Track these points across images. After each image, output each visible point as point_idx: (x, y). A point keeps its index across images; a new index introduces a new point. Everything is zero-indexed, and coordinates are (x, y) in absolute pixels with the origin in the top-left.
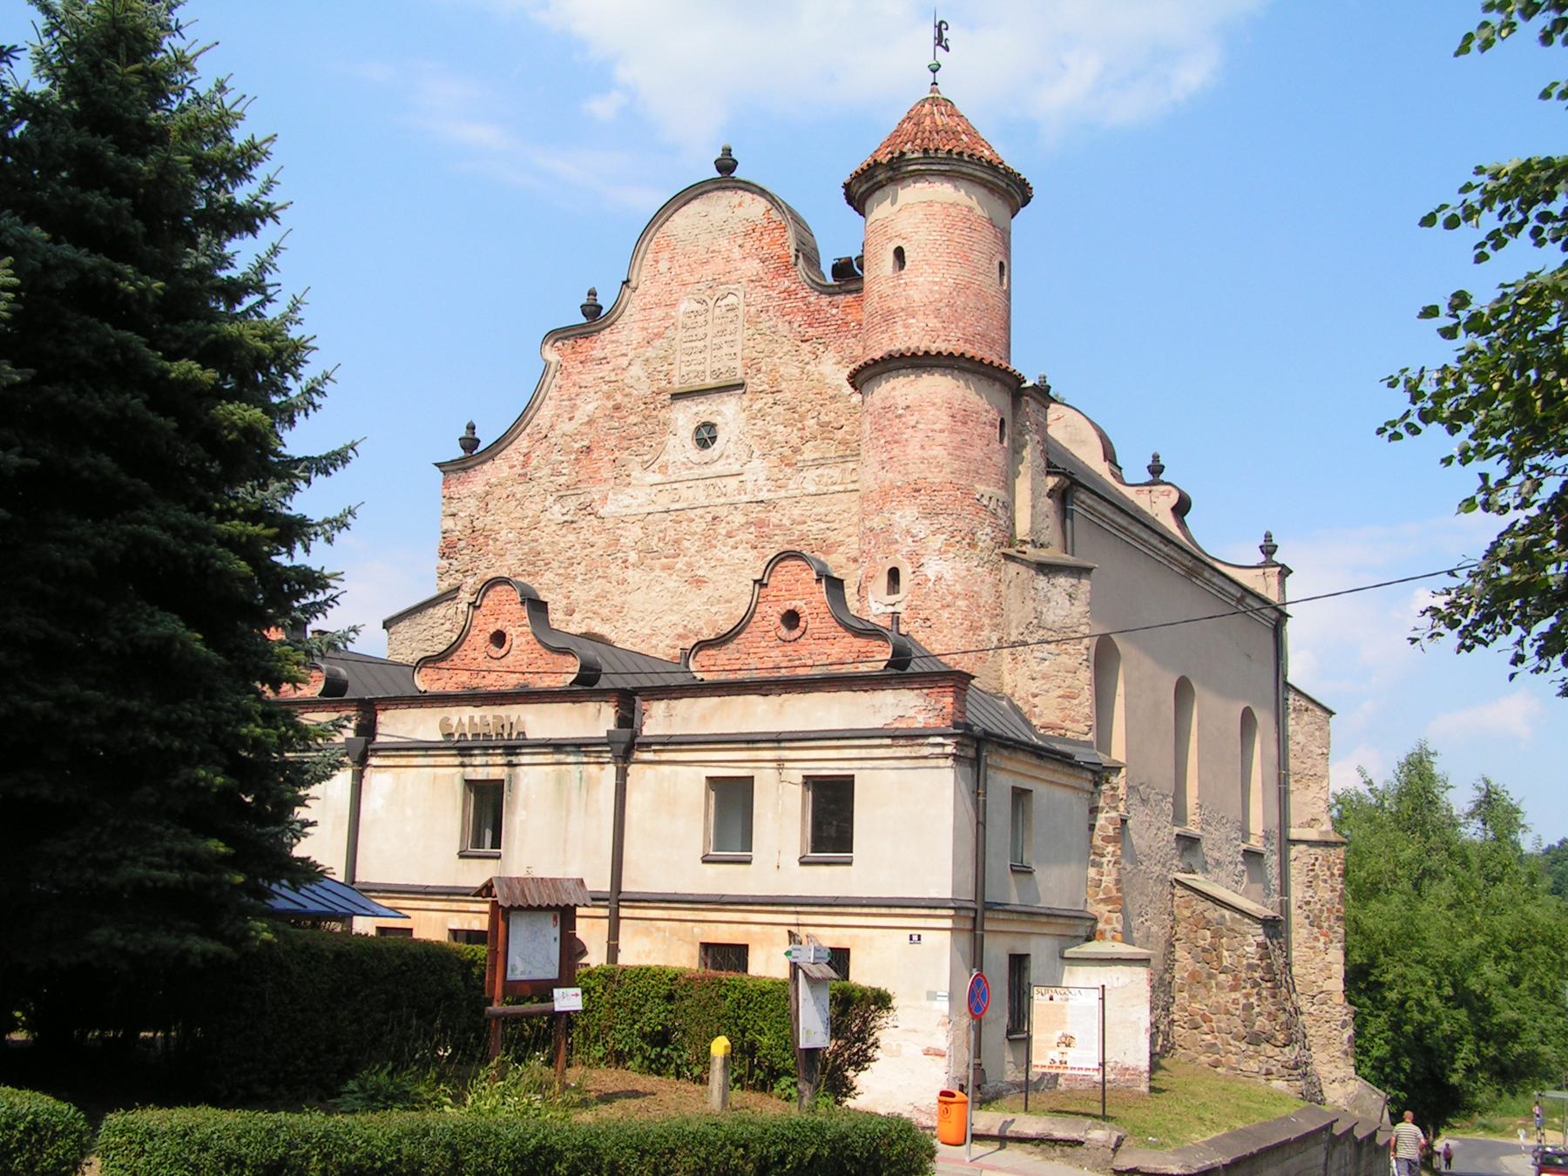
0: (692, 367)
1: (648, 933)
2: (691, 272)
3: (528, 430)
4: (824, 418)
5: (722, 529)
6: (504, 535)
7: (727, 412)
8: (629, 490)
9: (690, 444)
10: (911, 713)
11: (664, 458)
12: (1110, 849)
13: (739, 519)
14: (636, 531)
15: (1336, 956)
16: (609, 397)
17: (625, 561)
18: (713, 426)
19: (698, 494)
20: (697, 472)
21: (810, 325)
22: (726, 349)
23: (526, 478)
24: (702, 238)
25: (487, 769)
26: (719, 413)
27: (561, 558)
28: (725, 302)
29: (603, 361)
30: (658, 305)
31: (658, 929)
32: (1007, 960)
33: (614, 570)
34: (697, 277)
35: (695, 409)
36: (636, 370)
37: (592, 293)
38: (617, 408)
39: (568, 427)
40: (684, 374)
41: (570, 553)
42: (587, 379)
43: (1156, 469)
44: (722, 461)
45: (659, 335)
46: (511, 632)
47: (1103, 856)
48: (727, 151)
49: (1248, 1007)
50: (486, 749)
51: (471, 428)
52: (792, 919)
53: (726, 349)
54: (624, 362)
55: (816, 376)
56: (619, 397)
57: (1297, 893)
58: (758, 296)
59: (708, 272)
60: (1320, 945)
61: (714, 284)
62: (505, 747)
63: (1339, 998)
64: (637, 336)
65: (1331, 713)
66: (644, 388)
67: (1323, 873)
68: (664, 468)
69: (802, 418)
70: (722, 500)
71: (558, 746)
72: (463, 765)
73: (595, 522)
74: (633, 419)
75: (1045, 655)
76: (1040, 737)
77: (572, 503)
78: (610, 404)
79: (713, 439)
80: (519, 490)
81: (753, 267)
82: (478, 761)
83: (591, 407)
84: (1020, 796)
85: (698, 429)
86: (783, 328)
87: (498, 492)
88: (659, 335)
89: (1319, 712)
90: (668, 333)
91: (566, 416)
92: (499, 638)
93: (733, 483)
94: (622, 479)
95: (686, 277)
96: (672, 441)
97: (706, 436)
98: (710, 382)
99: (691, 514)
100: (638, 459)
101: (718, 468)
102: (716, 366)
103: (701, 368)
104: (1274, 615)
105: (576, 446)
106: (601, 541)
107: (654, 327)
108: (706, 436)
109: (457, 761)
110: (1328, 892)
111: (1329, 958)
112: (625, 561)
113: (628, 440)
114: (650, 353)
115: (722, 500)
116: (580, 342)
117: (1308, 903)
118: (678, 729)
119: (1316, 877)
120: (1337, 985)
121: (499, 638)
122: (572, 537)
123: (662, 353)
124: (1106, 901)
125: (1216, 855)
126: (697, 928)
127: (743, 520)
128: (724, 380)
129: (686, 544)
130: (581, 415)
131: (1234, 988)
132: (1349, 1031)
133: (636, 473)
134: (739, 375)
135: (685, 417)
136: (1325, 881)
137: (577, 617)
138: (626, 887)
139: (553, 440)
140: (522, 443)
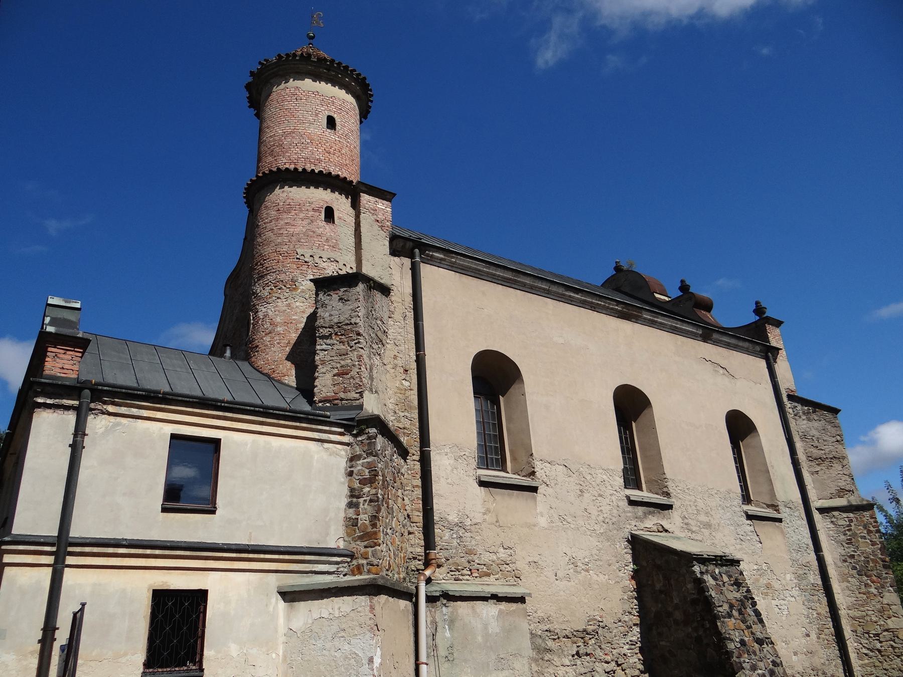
32: (150, 595)
43: (684, 287)
47: (358, 497)
60: (873, 590)
65: (835, 411)
75: (324, 347)
111: (885, 601)
117: (852, 557)
119: (855, 535)
124: (361, 538)
125: (703, 518)
136: (864, 538)
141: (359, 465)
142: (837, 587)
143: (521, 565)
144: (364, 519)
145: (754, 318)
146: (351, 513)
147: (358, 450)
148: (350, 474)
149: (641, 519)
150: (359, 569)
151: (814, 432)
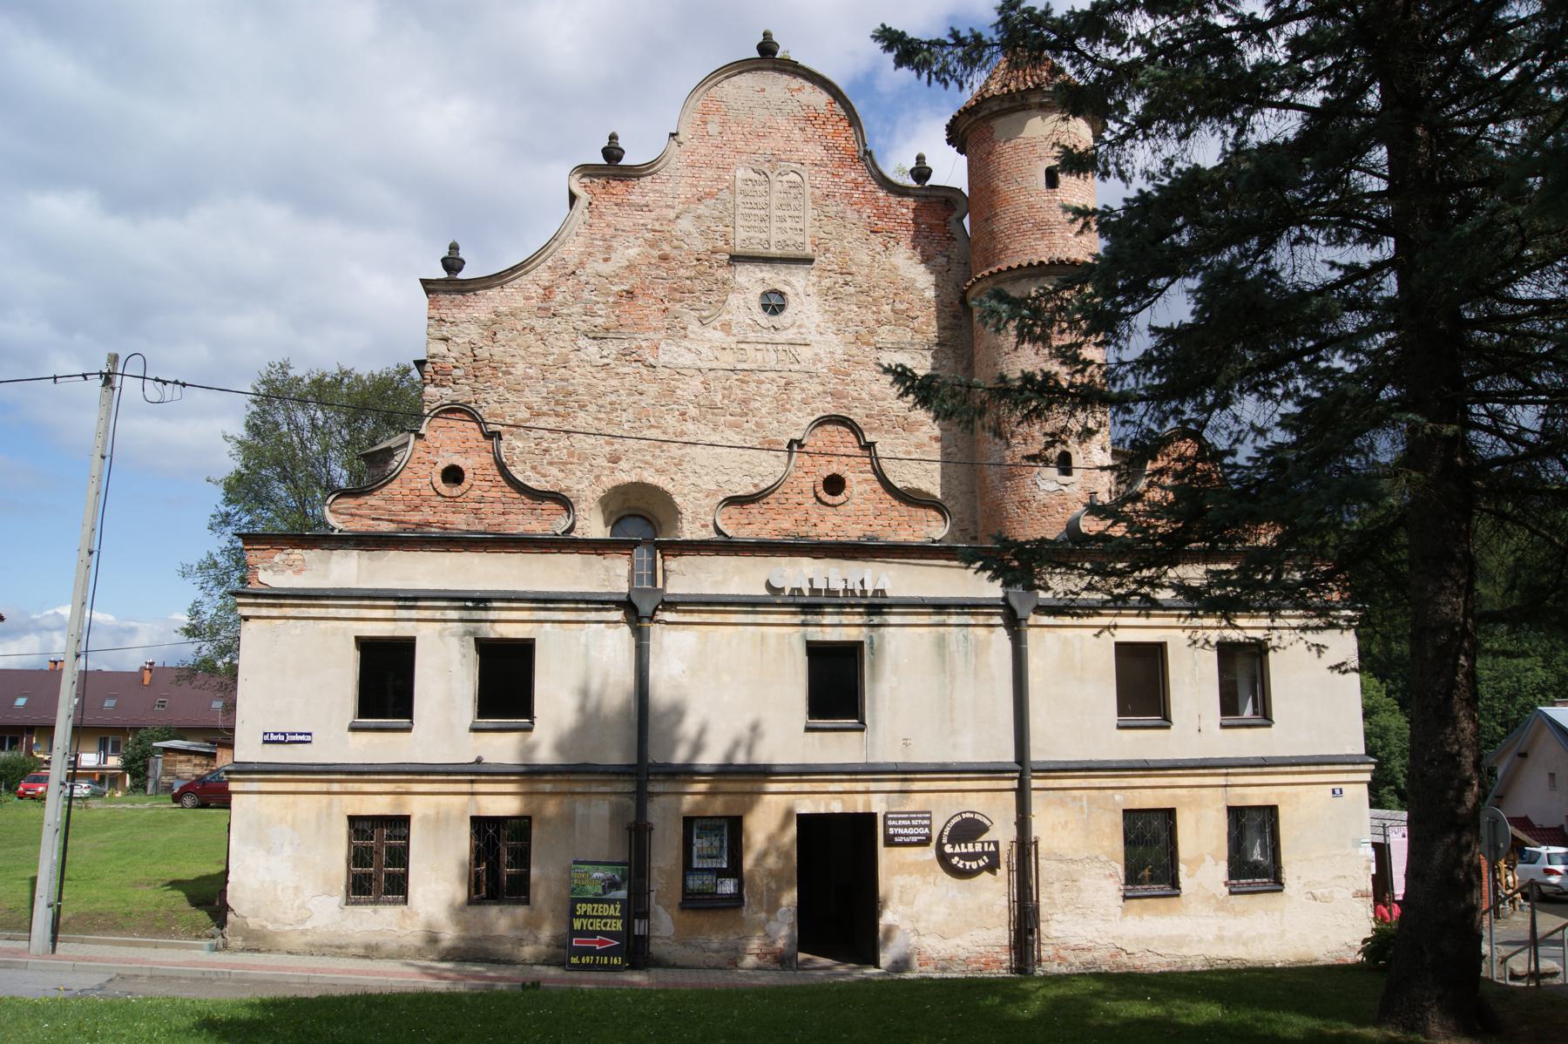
0: (752, 234)
1: (1062, 803)
2: (747, 143)
3: (549, 262)
4: (899, 306)
5: (797, 395)
6: (519, 370)
7: (795, 282)
8: (686, 343)
9: (757, 309)
11: (725, 317)
13: (814, 387)
14: (696, 384)
16: (653, 245)
17: (683, 414)
18: (782, 294)
19: (770, 358)
20: (767, 336)
21: (879, 218)
22: (789, 223)
24: (758, 111)
25: (836, 630)
26: (786, 283)
27: (600, 402)
28: (785, 178)
29: (640, 208)
30: (709, 165)
31: (1074, 799)
33: (671, 421)
34: (753, 148)
35: (760, 275)
36: (685, 224)
37: (613, 137)
38: (664, 258)
39: (605, 268)
40: (745, 238)
41: (613, 398)
42: (626, 223)
44: (794, 330)
45: (710, 195)
46: (851, 478)
48: (766, 35)
50: (840, 607)
52: (1221, 780)
53: (789, 223)
54: (672, 214)
55: (888, 266)
56: (667, 248)
58: (822, 180)
59: (768, 145)
61: (774, 159)
62: (865, 606)
64: (684, 191)
66: (699, 245)
68: (726, 327)
70: (796, 367)
71: (940, 607)
72: (804, 624)
73: (644, 371)
74: (682, 272)
77: (612, 348)
78: (656, 253)
79: (782, 307)
80: (539, 324)
81: (815, 152)
82: (827, 620)
83: (633, 252)
85: (765, 294)
86: (851, 215)
87: (508, 322)
88: (710, 195)
90: (721, 195)
91: (600, 256)
92: (835, 484)
93: (805, 353)
94: (676, 331)
95: (741, 144)
96: (734, 300)
97: (774, 303)
98: (774, 251)
99: (762, 376)
100: (696, 314)
101: (790, 335)
102: (782, 237)
103: (763, 236)
105: (615, 289)
106: (652, 389)
107: (704, 185)
108: (774, 303)
109: (799, 619)
112: (683, 414)
113: (679, 292)
114: (701, 209)
115: (796, 367)
116: (614, 183)
121: (835, 484)
122: (615, 382)
123: (716, 213)
126: (1118, 796)
127: (821, 389)
128: (791, 251)
129: (754, 405)
133: (694, 327)
134: (809, 250)
135: (752, 280)
137: (623, 464)
138: (1036, 755)
139: (583, 278)
140: (542, 274)
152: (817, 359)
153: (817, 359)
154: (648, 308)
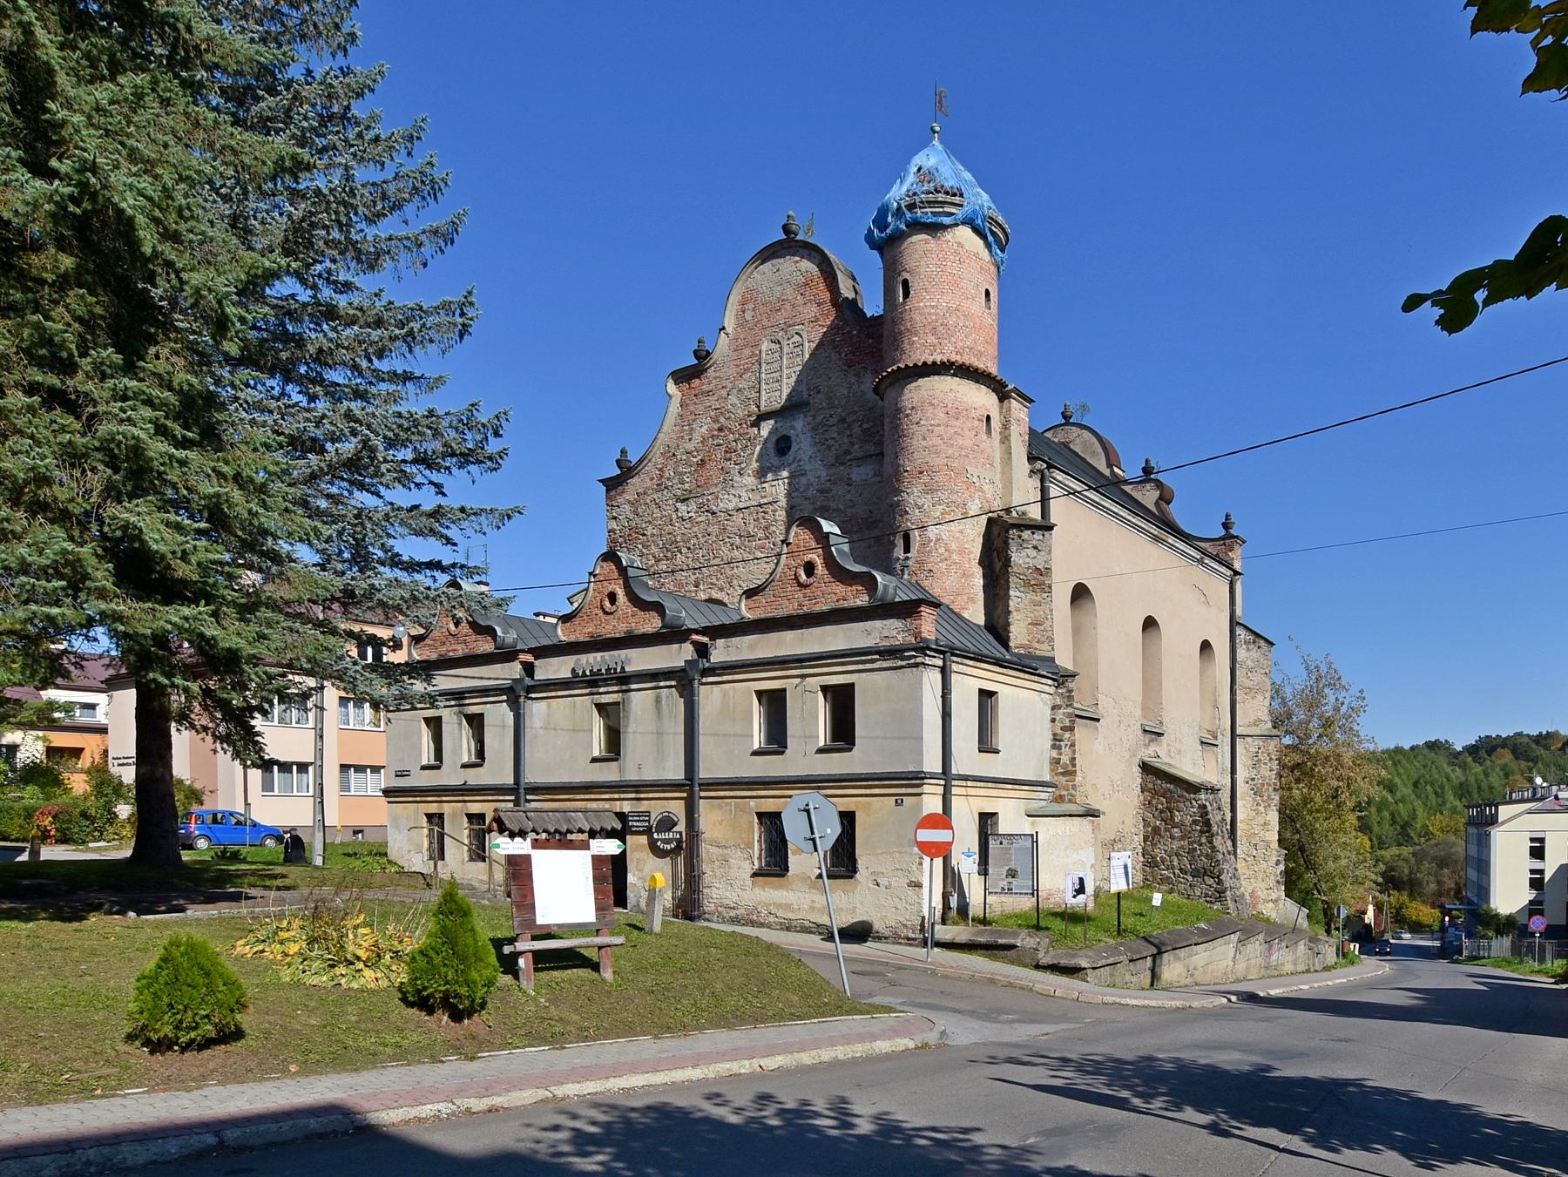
10: (894, 633)
12: (1067, 735)
15: (1273, 817)
23: (661, 487)
26: (792, 427)
36: (733, 399)
39: (690, 446)
49: (1191, 851)
51: (623, 452)
57: (1241, 775)
60: (1261, 809)
63: (1275, 845)
67: (1263, 757)
69: (850, 427)
76: (1019, 656)
79: (789, 448)
84: (986, 696)
85: (778, 441)
89: (1262, 643)
104: (1229, 573)
110: (1269, 772)
118: (734, 657)
120: (1274, 837)
124: (1063, 774)
130: (697, 437)
131: (1182, 838)
132: (1282, 867)
141: (1060, 714)
142: (1239, 803)
143: (1089, 787)
144: (1065, 759)
145: (1222, 532)
146: (1054, 754)
147: (1058, 701)
148: (1053, 720)
149: (1146, 746)
150: (1059, 799)
151: (1249, 663)
152: (809, 484)
153: (809, 484)
154: (712, 469)
